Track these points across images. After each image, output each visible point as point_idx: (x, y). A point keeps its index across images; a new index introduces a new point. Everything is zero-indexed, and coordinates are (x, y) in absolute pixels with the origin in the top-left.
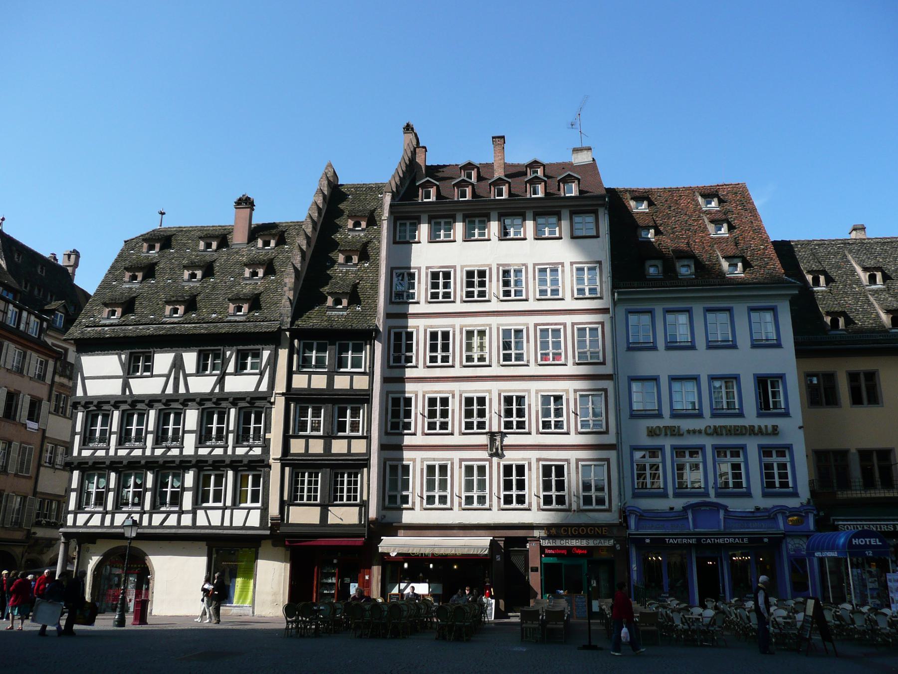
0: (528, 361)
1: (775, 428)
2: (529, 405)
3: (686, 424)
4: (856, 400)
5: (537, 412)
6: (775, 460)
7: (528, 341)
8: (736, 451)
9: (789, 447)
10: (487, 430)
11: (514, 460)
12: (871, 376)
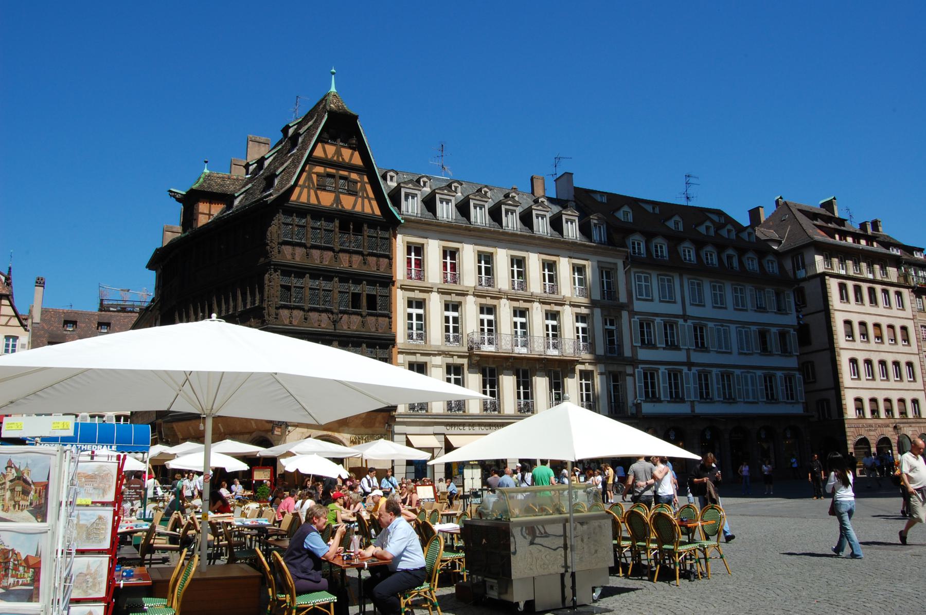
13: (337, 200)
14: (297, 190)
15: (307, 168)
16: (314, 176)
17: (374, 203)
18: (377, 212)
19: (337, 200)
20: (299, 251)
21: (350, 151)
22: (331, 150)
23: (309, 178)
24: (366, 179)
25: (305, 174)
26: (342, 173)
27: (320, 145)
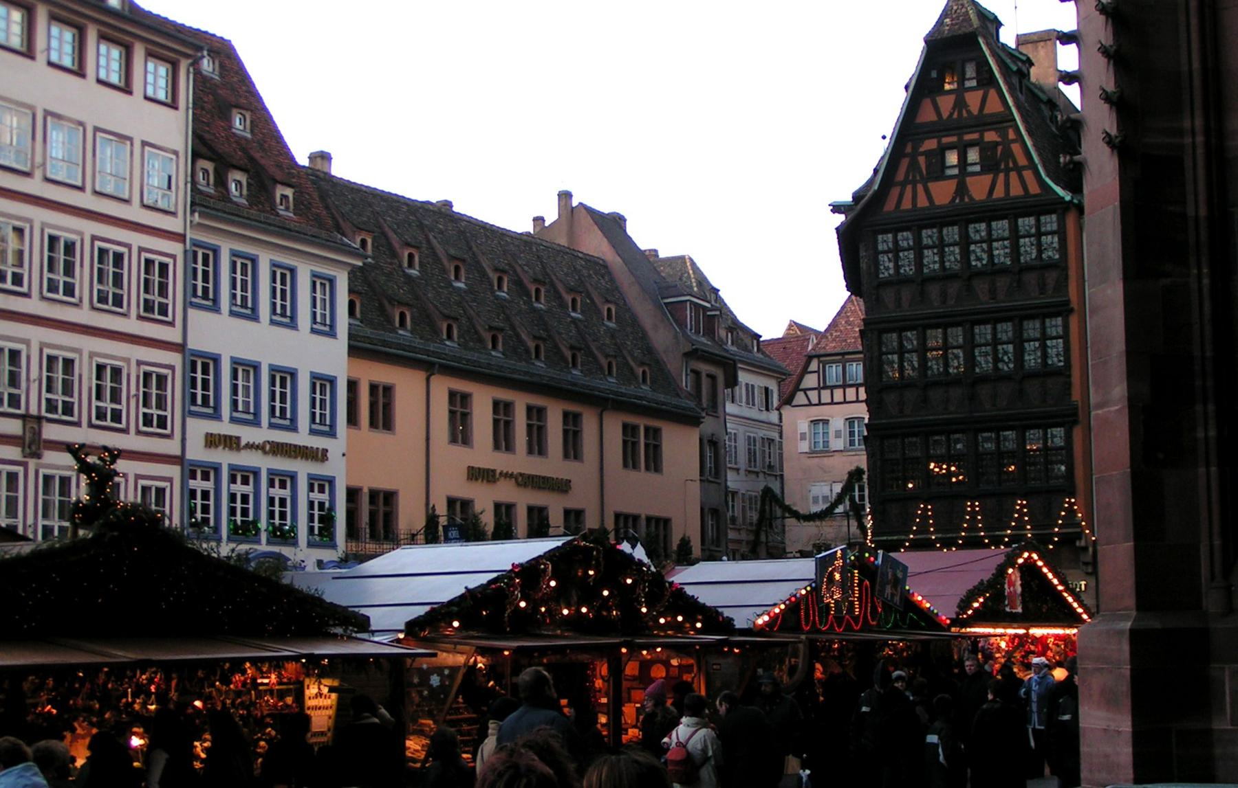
0: (81, 300)
1: (325, 451)
2: (80, 376)
3: (248, 434)
4: (373, 424)
5: (90, 389)
6: (198, 484)
7: (82, 265)
8: (286, 479)
9: (332, 481)
10: (22, 411)
11: (58, 468)
12: (388, 390)
13: (962, 189)
14: (895, 192)
15: (909, 149)
16: (922, 160)
17: (1027, 174)
18: (1034, 189)
19: (962, 189)
20: (906, 293)
21: (980, 93)
22: (946, 104)
23: (914, 165)
24: (1011, 135)
25: (905, 163)
26: (968, 137)
27: (927, 104)
